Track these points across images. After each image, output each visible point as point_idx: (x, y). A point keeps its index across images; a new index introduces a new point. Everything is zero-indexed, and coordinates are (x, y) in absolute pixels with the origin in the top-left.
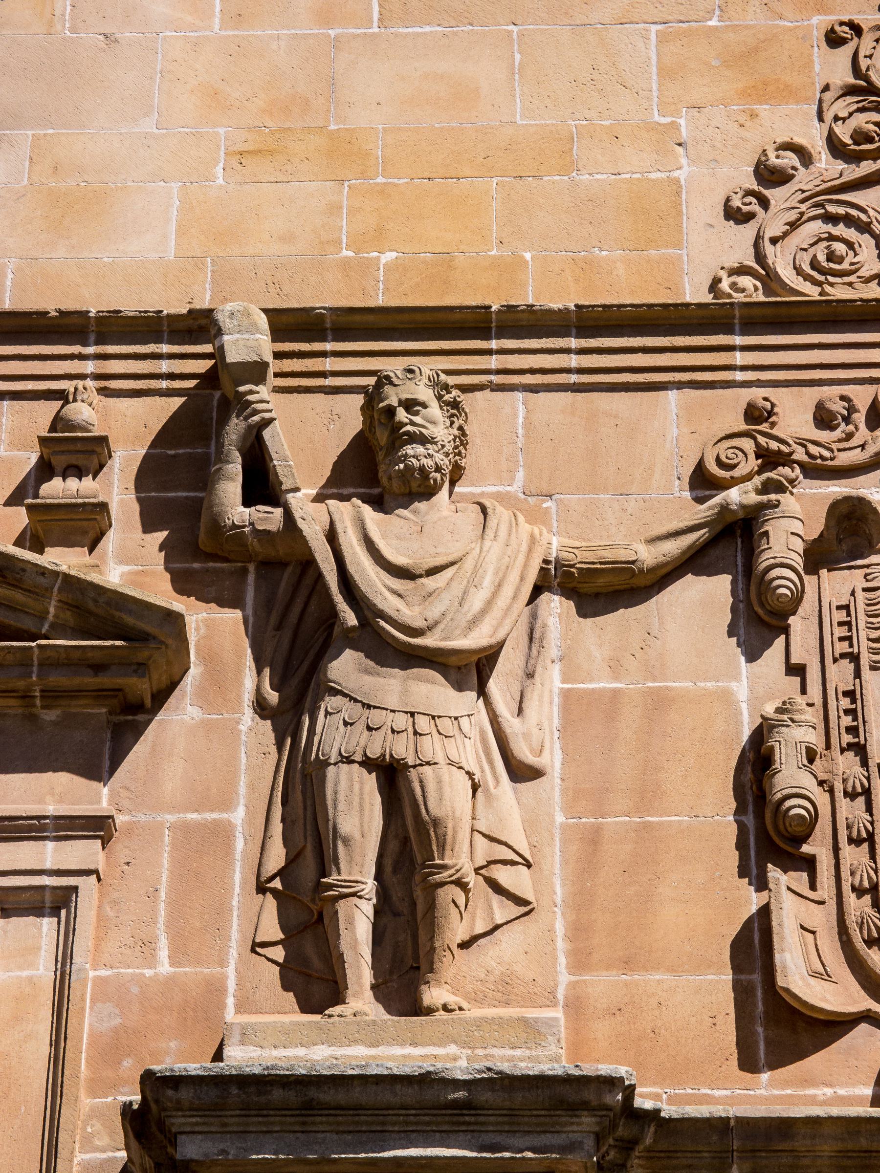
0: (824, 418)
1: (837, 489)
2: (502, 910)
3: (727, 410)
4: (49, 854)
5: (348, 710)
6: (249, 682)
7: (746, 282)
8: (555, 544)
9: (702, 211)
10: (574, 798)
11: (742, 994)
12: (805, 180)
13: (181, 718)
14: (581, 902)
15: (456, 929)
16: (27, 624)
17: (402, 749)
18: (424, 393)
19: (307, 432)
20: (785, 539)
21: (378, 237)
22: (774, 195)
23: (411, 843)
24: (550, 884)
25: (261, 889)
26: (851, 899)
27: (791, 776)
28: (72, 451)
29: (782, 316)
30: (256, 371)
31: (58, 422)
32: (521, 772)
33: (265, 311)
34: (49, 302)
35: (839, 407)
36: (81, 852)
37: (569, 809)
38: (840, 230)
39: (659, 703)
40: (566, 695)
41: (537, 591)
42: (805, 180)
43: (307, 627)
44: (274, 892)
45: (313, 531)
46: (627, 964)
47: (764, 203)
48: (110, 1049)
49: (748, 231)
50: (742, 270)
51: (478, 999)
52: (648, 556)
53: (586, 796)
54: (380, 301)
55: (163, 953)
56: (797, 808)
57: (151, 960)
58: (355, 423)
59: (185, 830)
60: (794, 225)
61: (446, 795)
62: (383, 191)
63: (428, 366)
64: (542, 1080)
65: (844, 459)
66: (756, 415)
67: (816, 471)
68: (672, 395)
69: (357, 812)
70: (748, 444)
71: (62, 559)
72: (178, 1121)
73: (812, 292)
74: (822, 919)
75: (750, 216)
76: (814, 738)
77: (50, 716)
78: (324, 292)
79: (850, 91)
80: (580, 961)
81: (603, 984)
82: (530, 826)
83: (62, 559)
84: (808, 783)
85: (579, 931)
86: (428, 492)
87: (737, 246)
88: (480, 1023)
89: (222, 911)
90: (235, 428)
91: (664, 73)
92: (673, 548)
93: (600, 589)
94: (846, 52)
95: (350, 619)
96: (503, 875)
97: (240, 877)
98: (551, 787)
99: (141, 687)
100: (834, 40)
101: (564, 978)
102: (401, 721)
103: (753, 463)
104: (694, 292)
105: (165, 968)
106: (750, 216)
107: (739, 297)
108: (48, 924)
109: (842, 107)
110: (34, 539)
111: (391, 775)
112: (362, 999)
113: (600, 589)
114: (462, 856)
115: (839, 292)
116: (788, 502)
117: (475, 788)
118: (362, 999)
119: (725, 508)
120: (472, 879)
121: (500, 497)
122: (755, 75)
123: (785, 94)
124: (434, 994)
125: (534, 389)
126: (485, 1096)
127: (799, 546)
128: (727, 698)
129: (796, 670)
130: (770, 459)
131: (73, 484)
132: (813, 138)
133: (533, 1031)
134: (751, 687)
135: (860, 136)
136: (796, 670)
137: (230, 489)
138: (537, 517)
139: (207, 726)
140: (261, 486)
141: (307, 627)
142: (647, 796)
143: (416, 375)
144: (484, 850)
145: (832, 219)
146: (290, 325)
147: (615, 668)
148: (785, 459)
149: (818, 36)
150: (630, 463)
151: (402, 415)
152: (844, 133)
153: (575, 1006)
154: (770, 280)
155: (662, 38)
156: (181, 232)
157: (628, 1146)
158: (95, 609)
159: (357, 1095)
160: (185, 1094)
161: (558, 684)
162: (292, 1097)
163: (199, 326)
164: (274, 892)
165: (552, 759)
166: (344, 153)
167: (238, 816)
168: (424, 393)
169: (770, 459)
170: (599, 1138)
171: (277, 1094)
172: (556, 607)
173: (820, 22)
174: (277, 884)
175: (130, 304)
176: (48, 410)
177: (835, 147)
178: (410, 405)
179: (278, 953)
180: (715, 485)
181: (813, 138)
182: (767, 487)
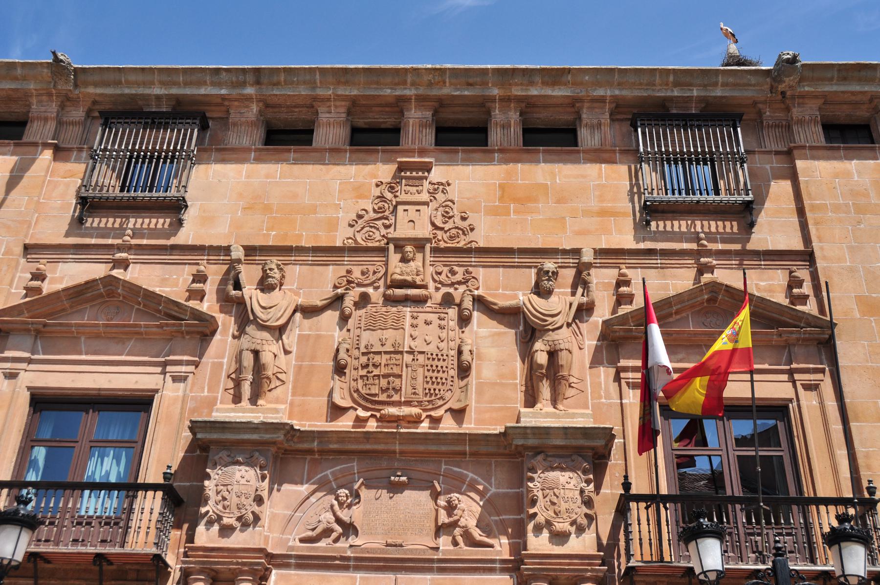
0: (363, 273)
1: (363, 289)
2: (278, 383)
3: (342, 271)
4: (184, 368)
5: (249, 338)
6: (231, 331)
7: (350, 241)
8: (300, 301)
9: (343, 224)
10: (298, 358)
11: (328, 401)
12: (366, 218)
13: (217, 337)
14: (296, 381)
15: (266, 388)
16: (183, 317)
17: (258, 348)
18: (274, 266)
19: (249, 274)
20: (348, 302)
21: (272, 229)
22: (360, 222)
23: (259, 367)
24: (290, 378)
25: (229, 377)
26: (352, 382)
27: (342, 355)
28: (200, 278)
29: (356, 250)
30: (239, 261)
31: (198, 271)
32: (287, 352)
33: (242, 246)
34: (198, 243)
35: (365, 270)
36: (191, 368)
37: (296, 361)
38: (373, 230)
39: (319, 337)
40: (299, 335)
41: (295, 311)
42: (366, 218)
43: (245, 319)
44: (232, 379)
45: (247, 297)
46: (304, 395)
47: (357, 222)
48: (193, 411)
49: (353, 229)
50: (350, 238)
51: (270, 402)
52: (320, 303)
53: (299, 358)
54: (270, 244)
55: (206, 390)
56: (343, 362)
57: (203, 392)
58: (261, 274)
59: (213, 364)
60: (362, 228)
61: (266, 357)
62: (275, 218)
63: (274, 259)
64: (272, 423)
65: (366, 282)
66: (349, 272)
67: (359, 285)
68: (331, 267)
69: (248, 360)
70: (345, 279)
71: (192, 304)
72: (197, 430)
73: (364, 244)
74: (345, 386)
75: (353, 226)
76: (348, 346)
77: (187, 337)
78: (257, 242)
79: (378, 197)
80: (293, 394)
81: (298, 399)
82: (287, 364)
83: (192, 304)
84: (345, 356)
85: (294, 388)
86: (274, 289)
87: (350, 232)
88: (267, 409)
89: (219, 382)
90: (233, 273)
91: (340, 192)
92: (325, 302)
93: (309, 311)
94: (379, 189)
95: (252, 318)
96: (279, 375)
97: (224, 375)
98: (293, 355)
99: (208, 332)
100: (377, 186)
101: (290, 398)
102: (259, 341)
103: (345, 283)
104: (339, 244)
105: (206, 394)
106: (353, 226)
107: (348, 245)
108: (182, 384)
109: (376, 201)
110: (188, 300)
111: (256, 353)
112: (245, 403)
113: (309, 311)
114: (269, 373)
115: (370, 245)
116: (351, 293)
117: (275, 356)
118: (245, 403)
119: (337, 294)
120: (271, 376)
121: (290, 290)
122: (359, 192)
123: (366, 197)
124: (260, 402)
125: (301, 265)
126: (260, 426)
127: (352, 303)
128: (333, 336)
129: (349, 330)
130: (349, 282)
131: (198, 285)
132: (370, 209)
133: (276, 411)
134: (337, 335)
135: (380, 208)
136: (349, 330)
137: (230, 287)
138: (297, 294)
139: (221, 340)
140: (238, 286)
141: (245, 319)
142: (313, 358)
143: (273, 261)
144: (276, 370)
145: (371, 227)
146: (250, 251)
147: (310, 329)
148: (353, 282)
149: (374, 185)
150: (321, 282)
151: (268, 271)
152: (376, 208)
153: (292, 404)
154: (355, 241)
155: (340, 184)
156: (230, 226)
157: (293, 436)
158: (198, 316)
159: (234, 425)
160: (198, 424)
161: (297, 332)
162: (221, 425)
163: (227, 250)
164: (232, 379)
165: (294, 349)
166: (267, 209)
167: (225, 360)
168: (274, 266)
169: (349, 282)
170: (285, 435)
171: (217, 425)
172: (298, 315)
173: (374, 181)
174: (233, 376)
175: (215, 243)
176: (195, 268)
177: (375, 211)
178: (271, 269)
179: (232, 391)
180: (338, 288)
181: (370, 208)
182: (347, 289)
